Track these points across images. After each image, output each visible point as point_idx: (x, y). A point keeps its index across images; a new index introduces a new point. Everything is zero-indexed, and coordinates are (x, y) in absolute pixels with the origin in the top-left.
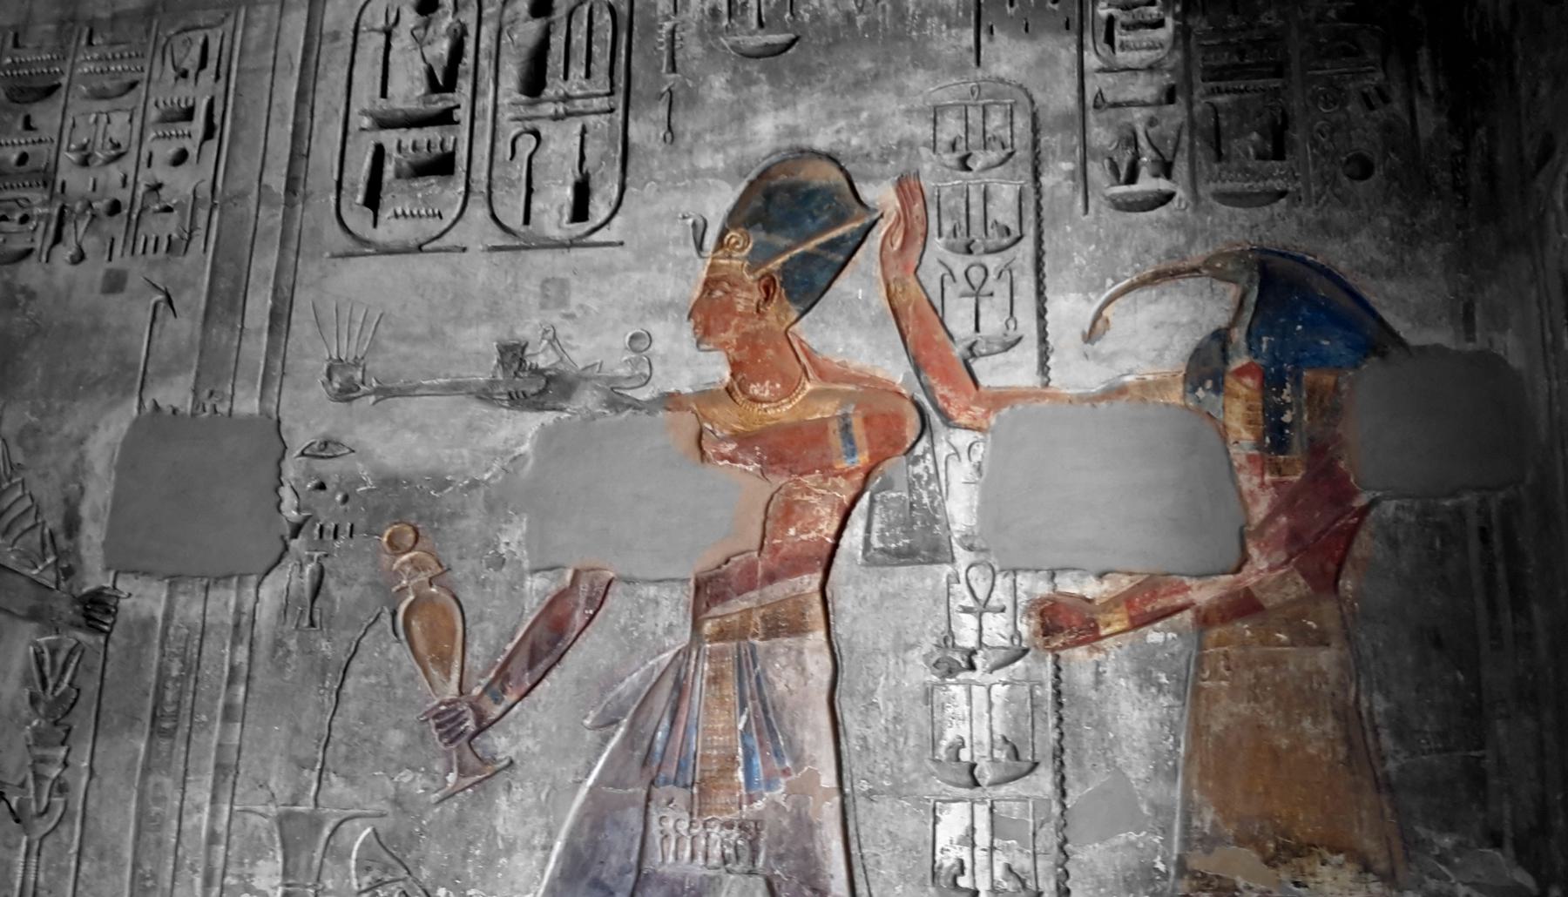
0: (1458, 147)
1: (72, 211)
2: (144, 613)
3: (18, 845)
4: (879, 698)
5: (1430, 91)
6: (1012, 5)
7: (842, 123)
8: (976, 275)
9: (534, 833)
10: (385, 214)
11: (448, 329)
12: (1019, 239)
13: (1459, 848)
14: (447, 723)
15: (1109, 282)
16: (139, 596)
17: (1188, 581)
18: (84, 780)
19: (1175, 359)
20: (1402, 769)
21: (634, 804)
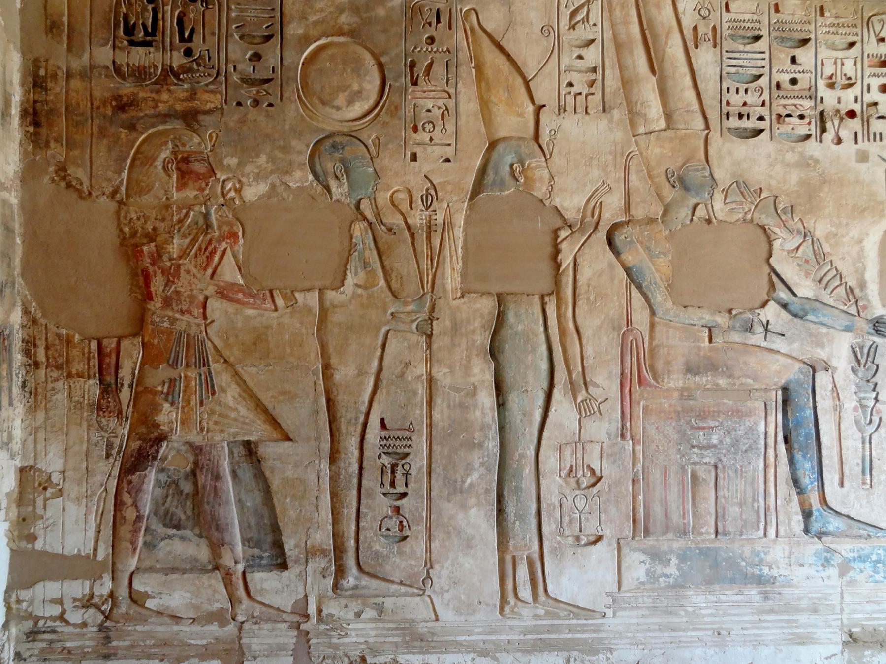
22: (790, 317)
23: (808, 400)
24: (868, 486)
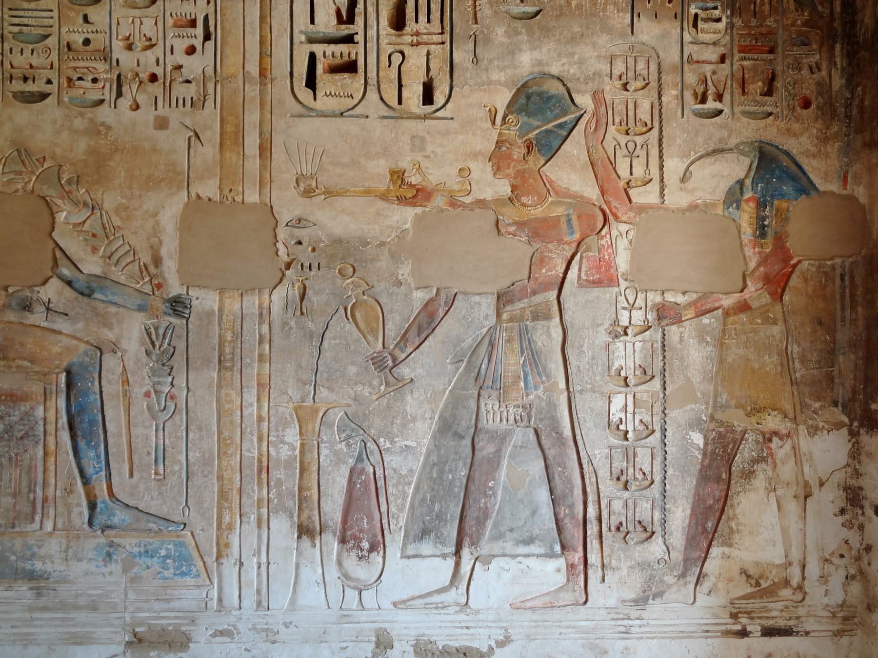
0: (849, 96)
1: (126, 78)
2: (207, 308)
3: (151, 426)
4: (585, 349)
5: (839, 67)
6: (649, 2)
7: (565, 60)
8: (631, 146)
9: (425, 412)
10: (320, 94)
11: (362, 160)
12: (651, 129)
13: (822, 408)
14: (378, 362)
15: (693, 153)
16: (203, 299)
17: (721, 296)
18: (185, 392)
19: (720, 194)
20: (802, 376)
21: (472, 398)
22: (74, 294)
23: (93, 384)
24: (162, 477)
